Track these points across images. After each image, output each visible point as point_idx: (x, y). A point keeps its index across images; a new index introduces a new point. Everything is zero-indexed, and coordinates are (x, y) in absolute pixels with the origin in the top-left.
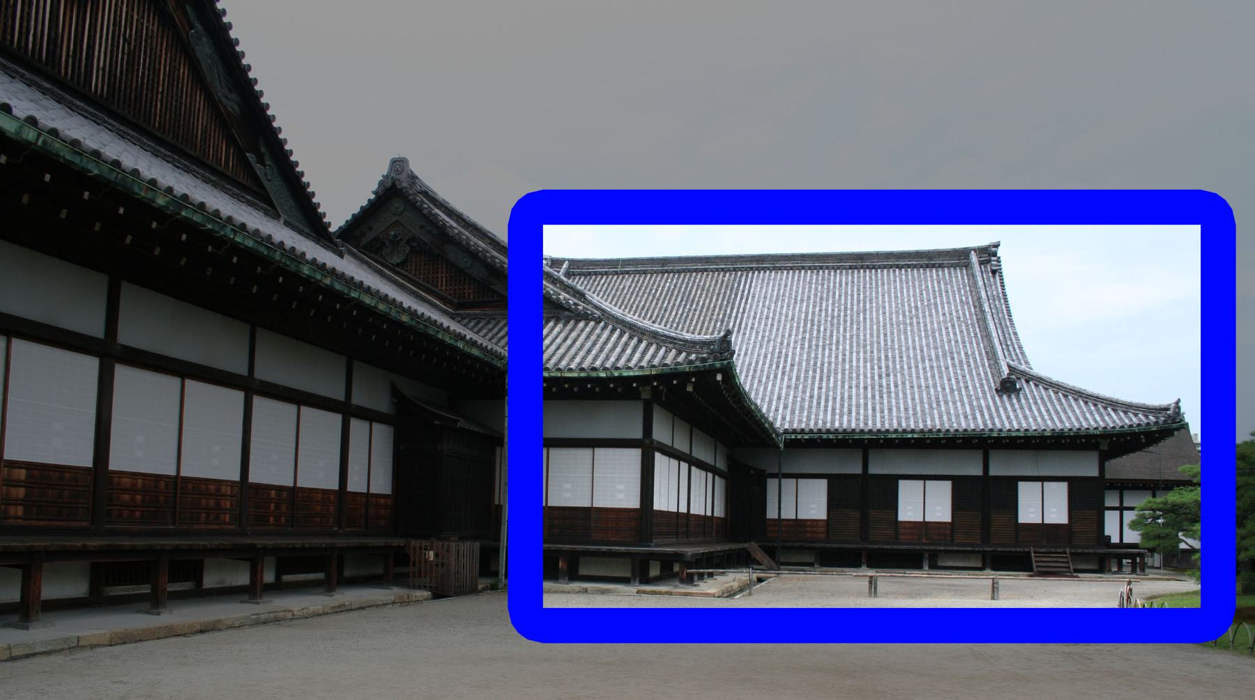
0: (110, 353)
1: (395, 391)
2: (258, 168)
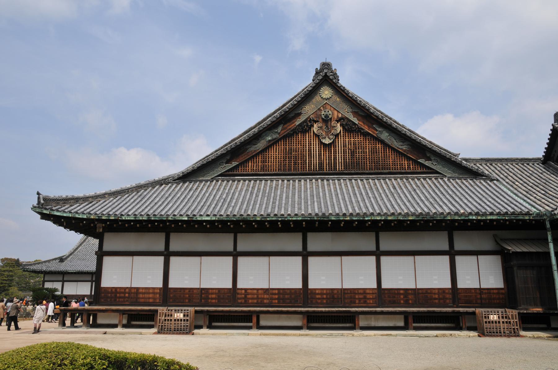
2: (427, 163)
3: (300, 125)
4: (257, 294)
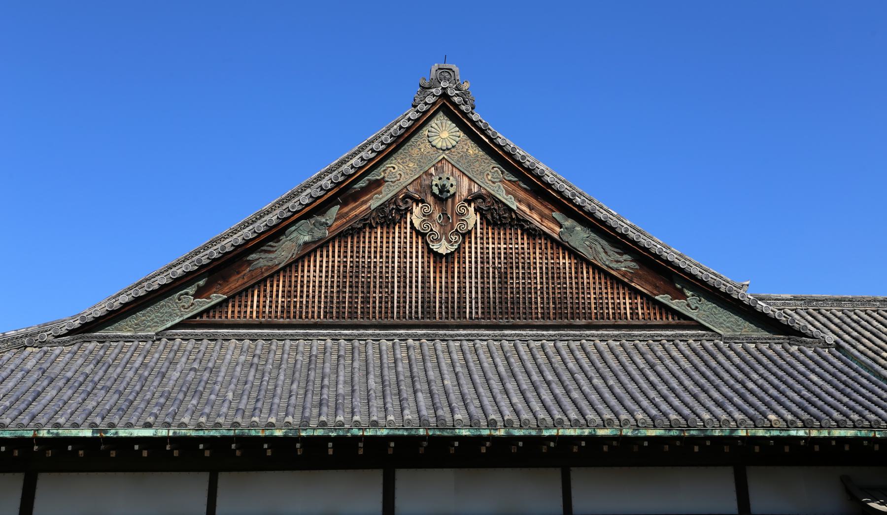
2: (675, 304)
3: (381, 208)
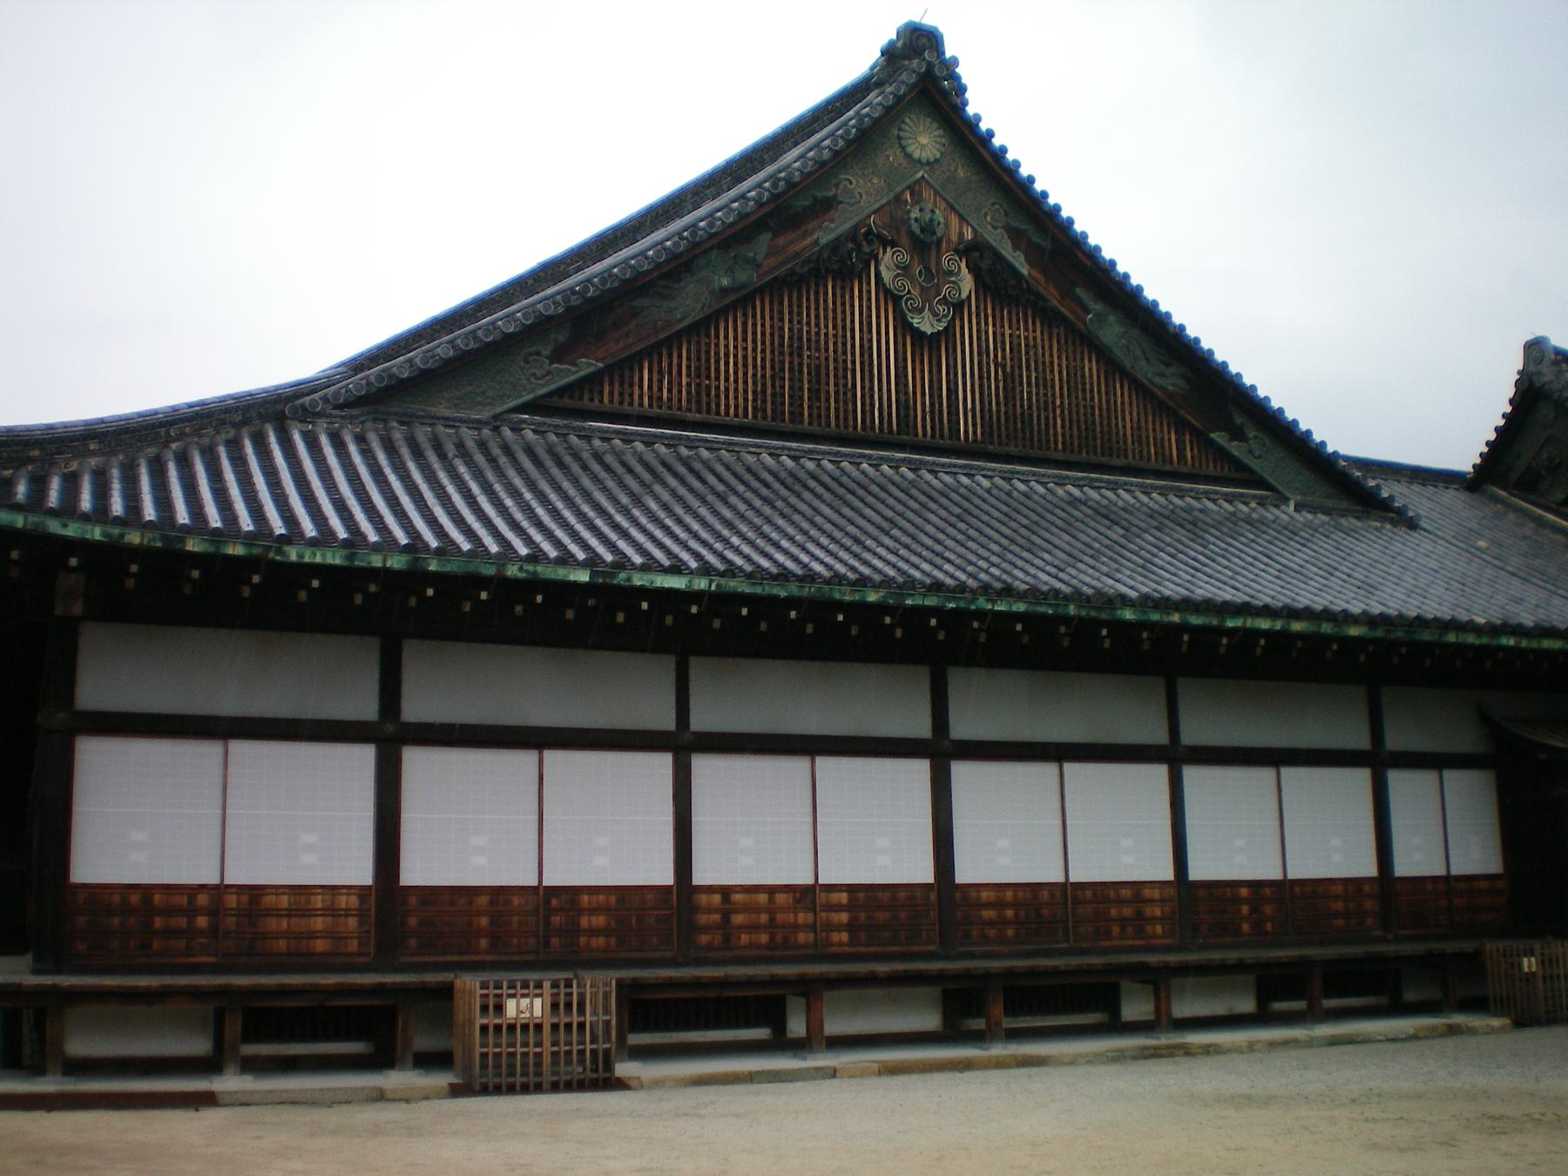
0: (941, 751)
1: (1485, 719)
2: (1235, 448)
3: (835, 246)
4: (771, 910)
